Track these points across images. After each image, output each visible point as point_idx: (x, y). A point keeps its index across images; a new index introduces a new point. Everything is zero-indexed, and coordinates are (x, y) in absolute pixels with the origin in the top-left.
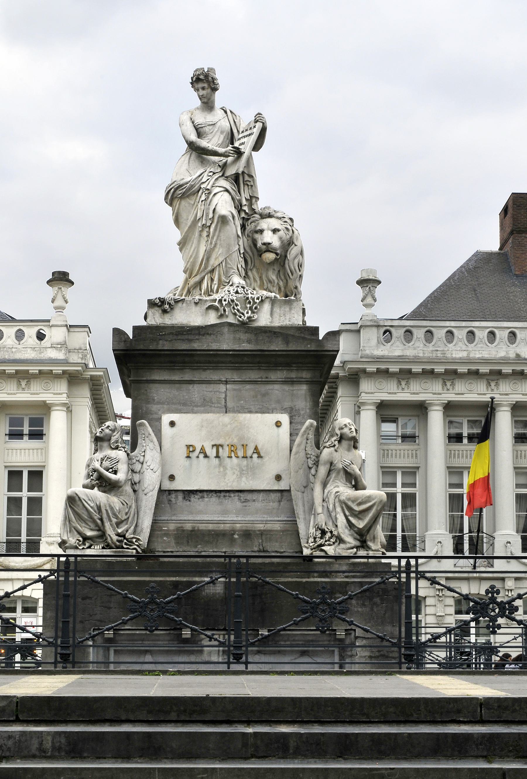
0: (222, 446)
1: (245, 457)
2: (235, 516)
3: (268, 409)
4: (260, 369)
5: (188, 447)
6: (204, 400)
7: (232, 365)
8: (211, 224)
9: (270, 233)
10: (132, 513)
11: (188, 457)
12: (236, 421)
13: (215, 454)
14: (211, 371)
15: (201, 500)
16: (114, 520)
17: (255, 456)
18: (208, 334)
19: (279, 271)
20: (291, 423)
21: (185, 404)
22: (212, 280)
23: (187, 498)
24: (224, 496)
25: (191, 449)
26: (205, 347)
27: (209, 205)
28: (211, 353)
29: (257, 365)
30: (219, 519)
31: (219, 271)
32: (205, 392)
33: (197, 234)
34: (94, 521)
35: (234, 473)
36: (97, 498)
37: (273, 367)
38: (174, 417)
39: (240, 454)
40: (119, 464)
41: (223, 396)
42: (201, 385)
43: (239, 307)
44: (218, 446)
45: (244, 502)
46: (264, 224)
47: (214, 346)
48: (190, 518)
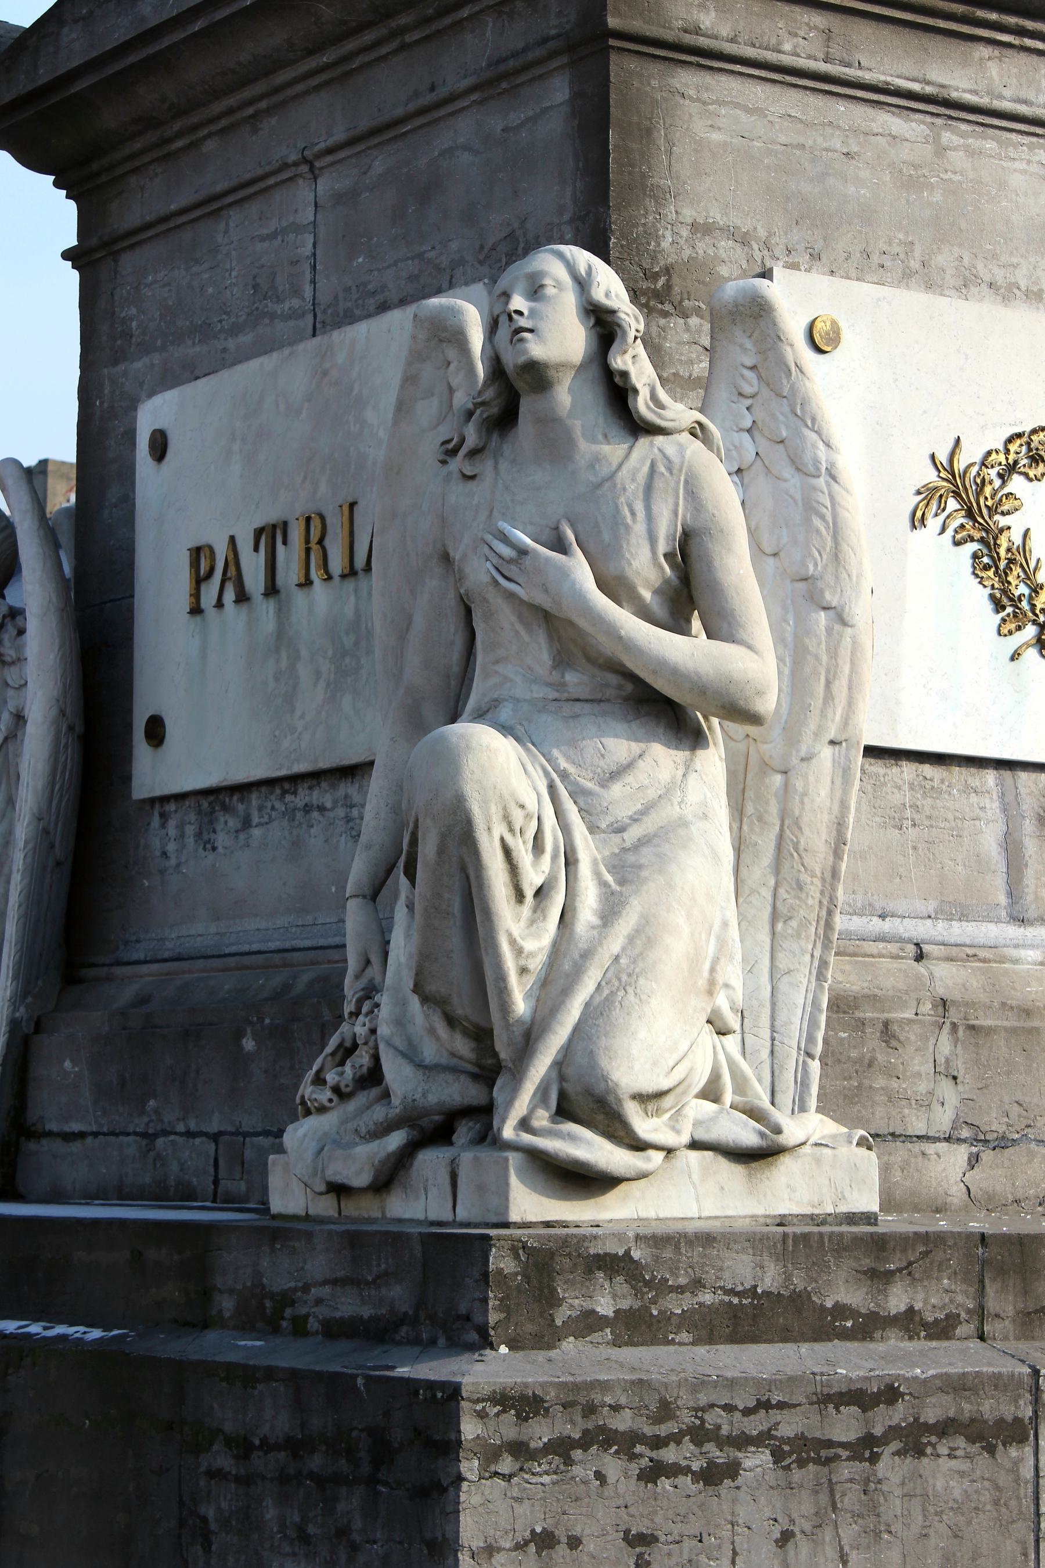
1: (351, 573)
3: (438, 269)
6: (256, 287)
7: (312, 63)
14: (274, 121)
15: (242, 836)
21: (204, 332)
23: (206, 836)
24: (307, 809)
32: (259, 246)
35: (318, 674)
44: (270, 535)
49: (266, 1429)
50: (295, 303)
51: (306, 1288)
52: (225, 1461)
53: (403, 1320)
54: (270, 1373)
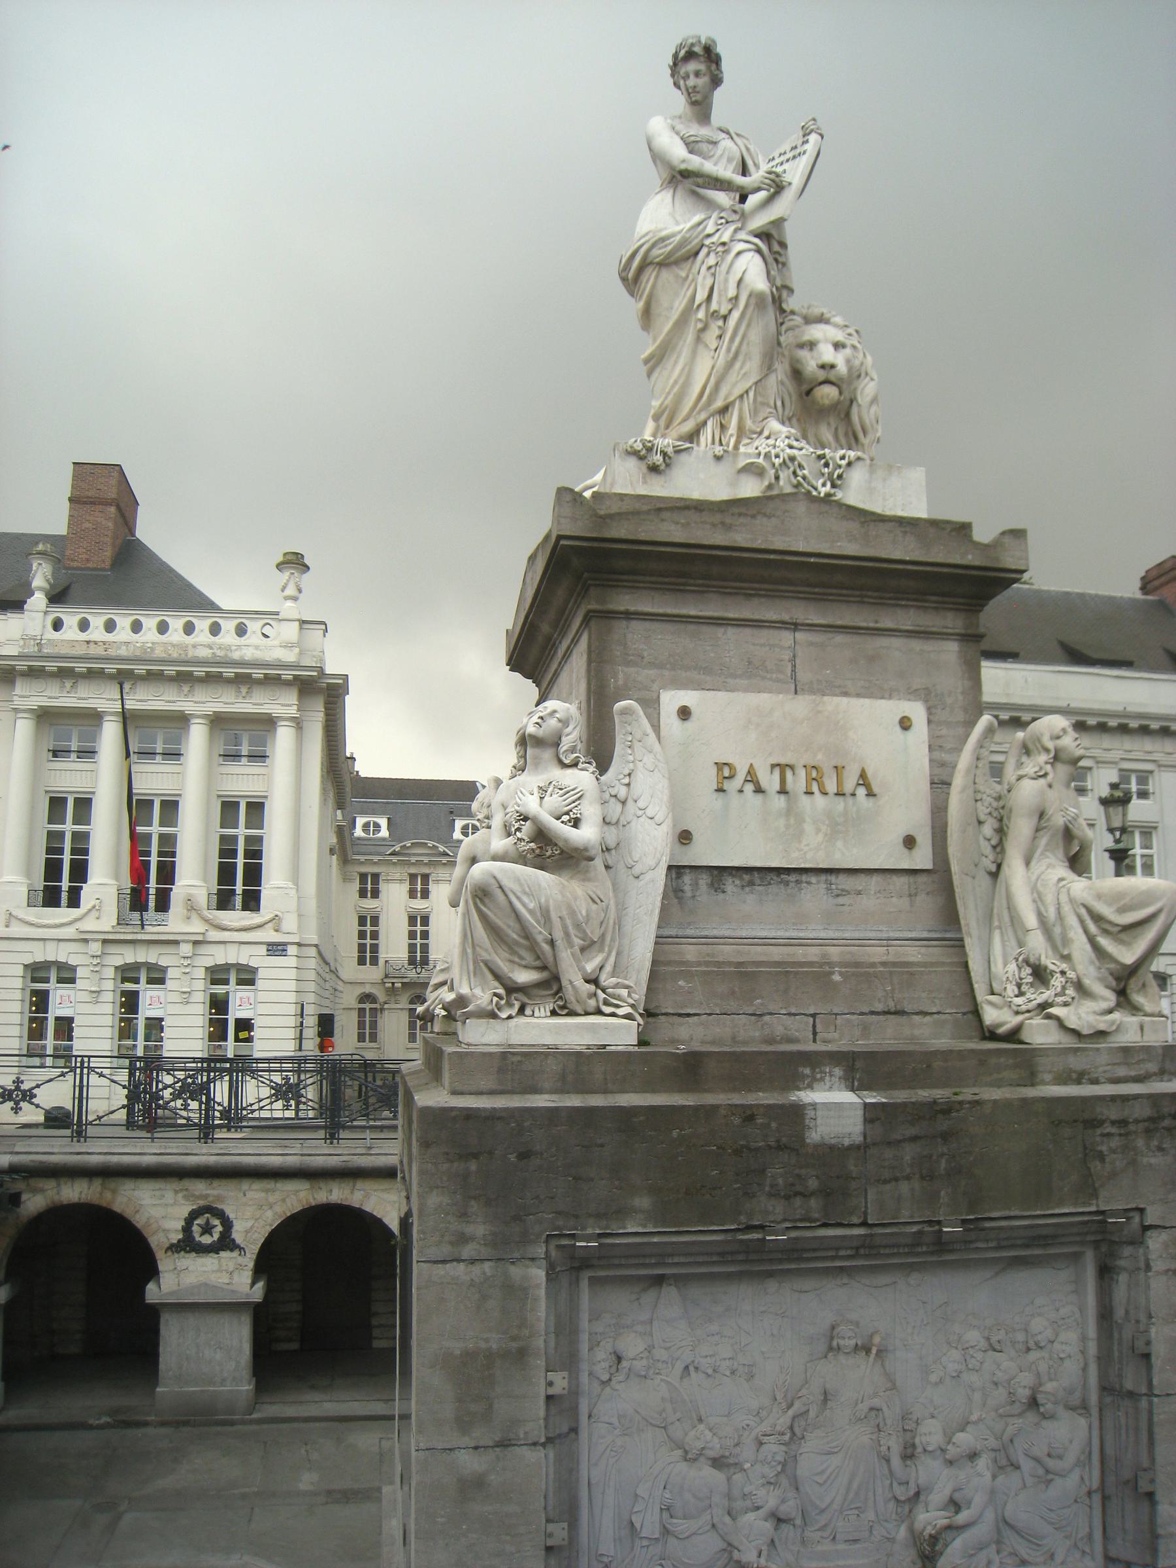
0: (792, 767)
1: (839, 794)
2: (820, 927)
4: (863, 602)
5: (720, 766)
6: (750, 663)
8: (730, 311)
9: (831, 348)
10: (611, 922)
11: (720, 790)
12: (819, 712)
13: (777, 787)
14: (763, 600)
15: (747, 889)
16: (578, 942)
17: (861, 791)
18: (765, 515)
19: (836, 429)
20: (929, 722)
21: (707, 670)
22: (723, 428)
25: (726, 773)
26: (759, 544)
27: (728, 273)
28: (772, 557)
29: (858, 593)
30: (788, 934)
31: (741, 410)
33: (690, 337)
34: (533, 947)
35: (818, 830)
36: (539, 886)
37: (890, 599)
38: (687, 697)
39: (831, 787)
40: (584, 802)
41: (787, 655)
42: (741, 629)
43: (805, 472)
44: (782, 768)
45: (838, 896)
46: (816, 332)
47: (779, 543)
48: (727, 933)
49: (1136, 1116)
50: (781, 676)
51: (1096, 1067)
52: (1113, 1130)
53: (1155, 1074)
54: (1136, 1097)
